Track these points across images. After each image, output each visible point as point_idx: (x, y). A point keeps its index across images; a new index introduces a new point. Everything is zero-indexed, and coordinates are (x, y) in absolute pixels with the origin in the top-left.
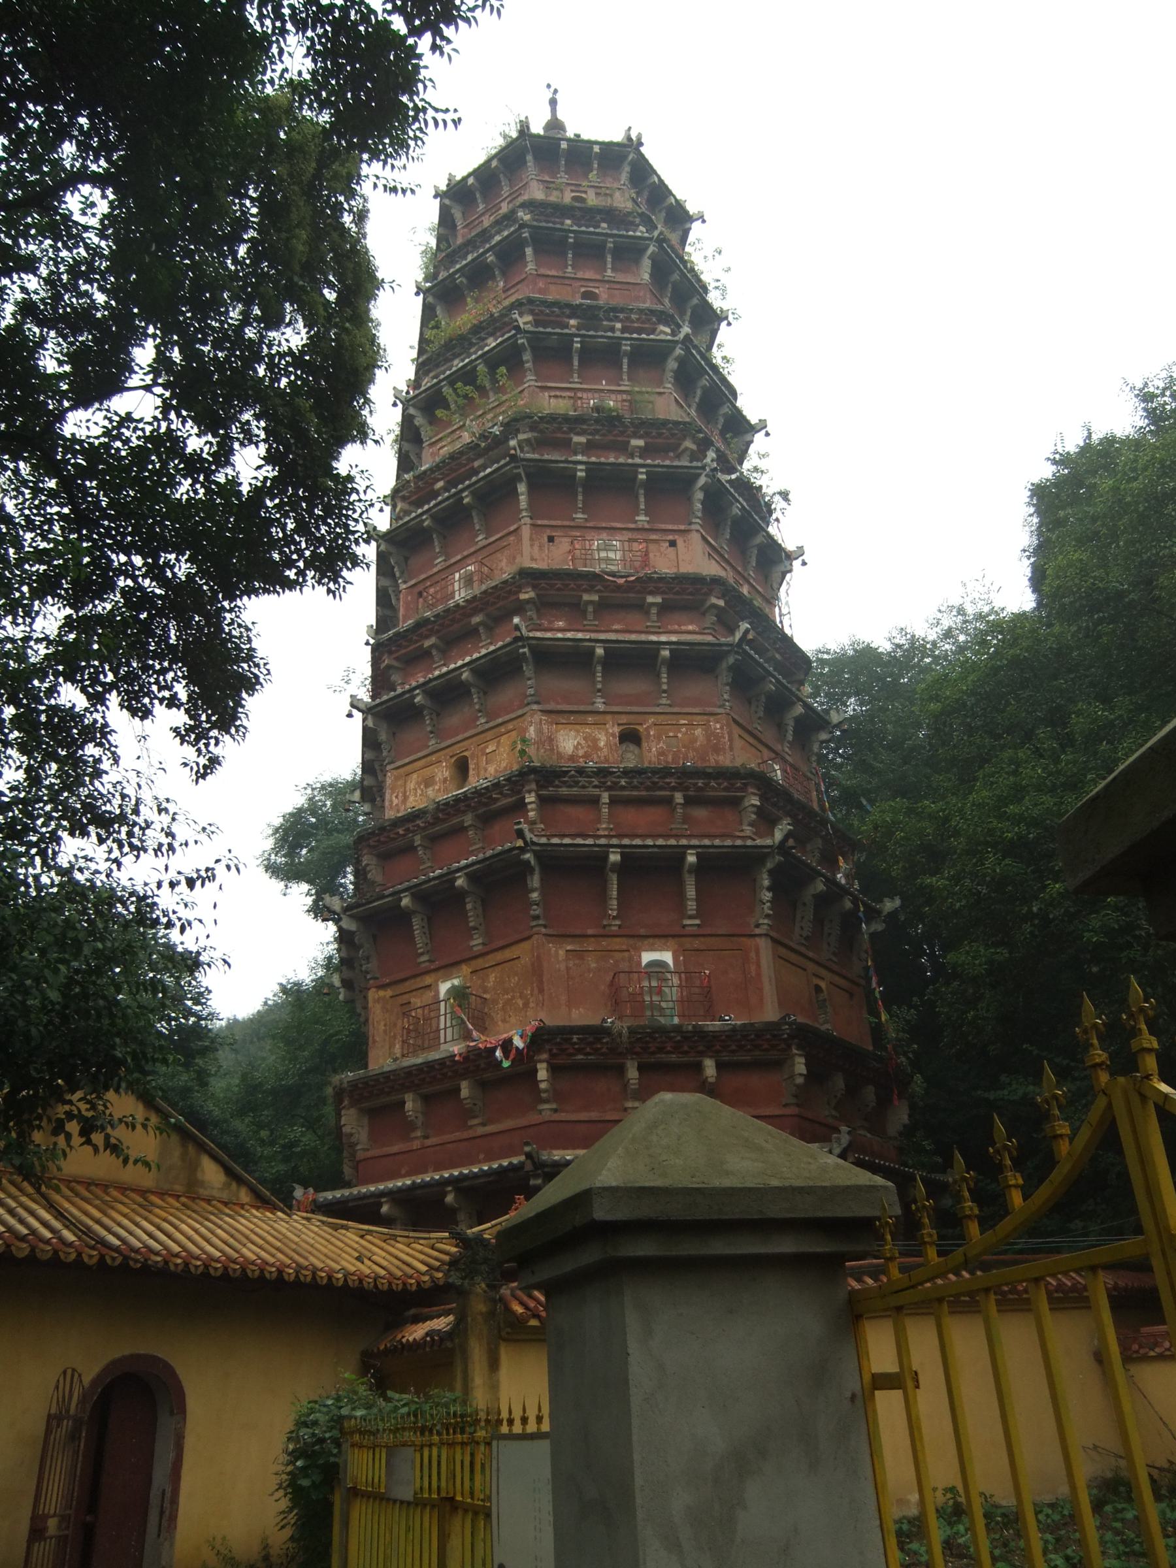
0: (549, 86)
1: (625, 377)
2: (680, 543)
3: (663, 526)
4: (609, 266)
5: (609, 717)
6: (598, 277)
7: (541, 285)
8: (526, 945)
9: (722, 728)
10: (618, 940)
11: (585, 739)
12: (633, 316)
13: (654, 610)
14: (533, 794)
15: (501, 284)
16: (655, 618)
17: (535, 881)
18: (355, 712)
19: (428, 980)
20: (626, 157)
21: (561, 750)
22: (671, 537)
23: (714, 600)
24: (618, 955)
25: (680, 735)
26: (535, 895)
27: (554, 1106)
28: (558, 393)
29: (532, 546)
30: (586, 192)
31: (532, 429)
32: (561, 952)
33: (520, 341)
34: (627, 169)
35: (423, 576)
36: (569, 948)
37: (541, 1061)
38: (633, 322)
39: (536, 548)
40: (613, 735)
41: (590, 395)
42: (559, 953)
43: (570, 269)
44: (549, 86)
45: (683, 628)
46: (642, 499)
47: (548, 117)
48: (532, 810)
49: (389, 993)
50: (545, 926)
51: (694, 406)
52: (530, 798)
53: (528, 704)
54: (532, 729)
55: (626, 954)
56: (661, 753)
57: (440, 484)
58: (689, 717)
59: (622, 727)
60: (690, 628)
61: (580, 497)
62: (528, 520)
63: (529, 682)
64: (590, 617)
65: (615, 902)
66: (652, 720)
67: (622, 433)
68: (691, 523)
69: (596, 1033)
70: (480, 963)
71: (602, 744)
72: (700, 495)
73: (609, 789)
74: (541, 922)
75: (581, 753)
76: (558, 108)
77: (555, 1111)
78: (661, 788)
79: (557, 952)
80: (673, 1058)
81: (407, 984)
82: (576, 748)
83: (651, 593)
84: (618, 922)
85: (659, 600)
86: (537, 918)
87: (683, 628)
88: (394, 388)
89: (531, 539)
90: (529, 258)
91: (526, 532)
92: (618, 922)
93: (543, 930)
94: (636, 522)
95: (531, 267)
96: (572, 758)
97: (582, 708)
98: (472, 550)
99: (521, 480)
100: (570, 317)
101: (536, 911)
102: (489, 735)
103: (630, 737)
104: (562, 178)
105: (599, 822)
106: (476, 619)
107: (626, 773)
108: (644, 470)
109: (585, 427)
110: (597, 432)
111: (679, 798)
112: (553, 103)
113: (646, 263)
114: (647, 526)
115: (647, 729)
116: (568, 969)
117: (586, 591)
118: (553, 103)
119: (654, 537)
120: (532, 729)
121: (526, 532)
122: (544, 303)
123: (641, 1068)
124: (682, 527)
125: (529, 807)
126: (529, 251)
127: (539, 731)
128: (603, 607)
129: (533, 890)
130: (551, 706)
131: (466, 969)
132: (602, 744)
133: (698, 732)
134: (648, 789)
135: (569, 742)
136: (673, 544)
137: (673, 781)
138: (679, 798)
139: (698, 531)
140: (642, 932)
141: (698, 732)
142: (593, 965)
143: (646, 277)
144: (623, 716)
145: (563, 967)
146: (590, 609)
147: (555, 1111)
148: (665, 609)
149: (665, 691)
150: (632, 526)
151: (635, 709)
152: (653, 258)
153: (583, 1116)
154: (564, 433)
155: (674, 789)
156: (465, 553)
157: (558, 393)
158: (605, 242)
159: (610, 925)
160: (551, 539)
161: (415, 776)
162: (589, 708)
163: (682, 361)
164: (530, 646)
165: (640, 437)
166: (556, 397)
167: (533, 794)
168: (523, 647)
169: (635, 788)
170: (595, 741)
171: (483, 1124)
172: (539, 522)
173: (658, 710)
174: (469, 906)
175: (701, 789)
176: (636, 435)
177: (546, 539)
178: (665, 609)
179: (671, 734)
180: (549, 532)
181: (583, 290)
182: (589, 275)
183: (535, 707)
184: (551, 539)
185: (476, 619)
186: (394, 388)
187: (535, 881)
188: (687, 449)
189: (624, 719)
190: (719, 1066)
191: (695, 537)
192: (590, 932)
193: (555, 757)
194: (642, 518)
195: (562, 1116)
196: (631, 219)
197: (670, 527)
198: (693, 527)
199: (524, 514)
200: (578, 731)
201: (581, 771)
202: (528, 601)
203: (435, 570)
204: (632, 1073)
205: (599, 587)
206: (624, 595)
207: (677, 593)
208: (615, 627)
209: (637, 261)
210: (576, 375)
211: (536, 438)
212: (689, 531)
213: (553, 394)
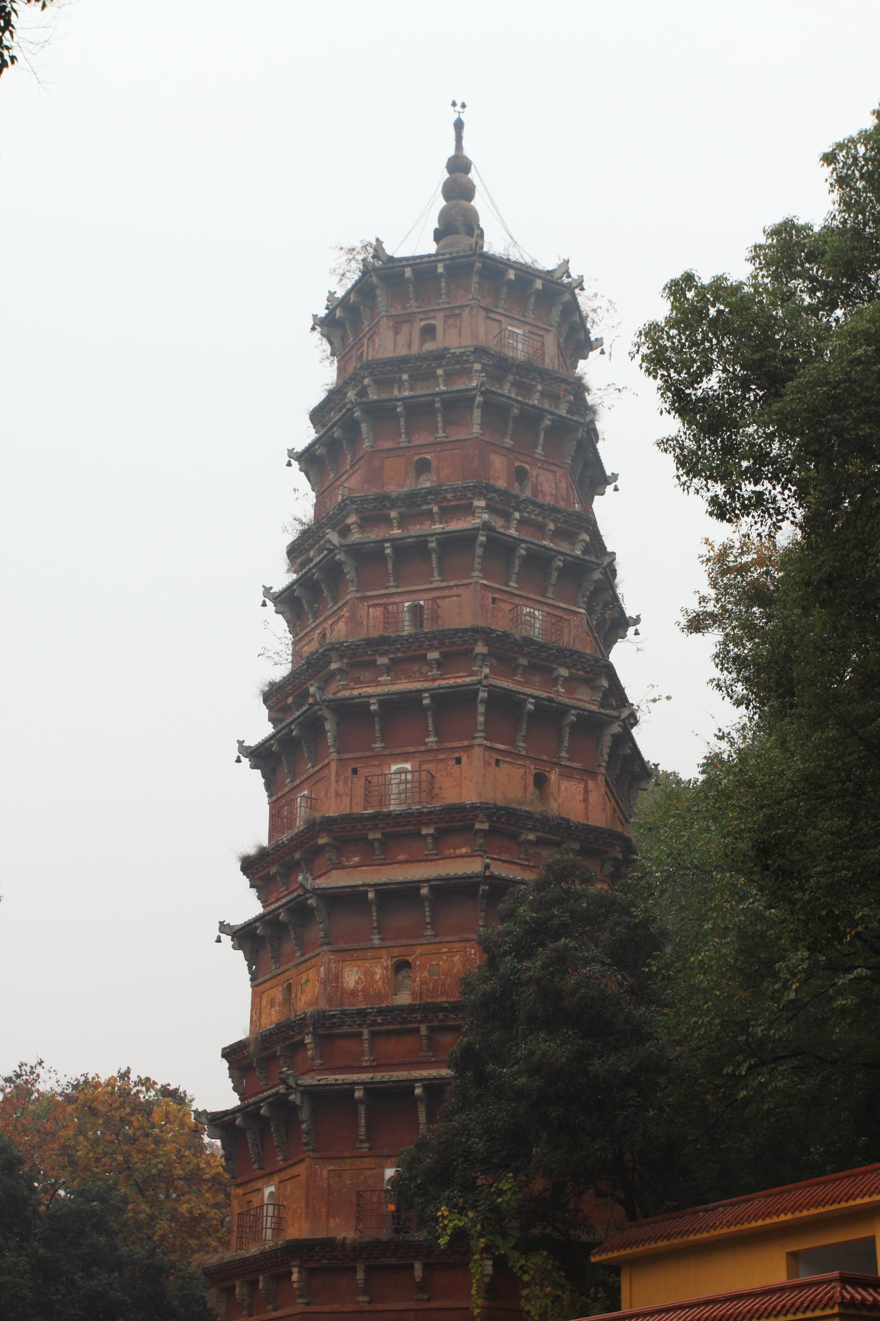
0: (454, 104)
1: (436, 573)
2: (464, 760)
3: (449, 745)
4: (440, 426)
5: (384, 951)
6: (431, 440)
7: (376, 463)
8: (304, 1165)
9: (475, 953)
10: (367, 1160)
11: (365, 974)
12: (449, 496)
13: (430, 840)
14: (310, 1036)
15: (349, 457)
16: (431, 847)
17: (305, 1114)
18: (224, 937)
19: (259, 1184)
20: (472, 265)
21: (345, 986)
22: (457, 755)
23: (478, 826)
24: (368, 1173)
25: (441, 963)
26: (304, 1126)
27: (306, 1301)
28: (376, 602)
29: (337, 782)
30: (435, 317)
31: (341, 657)
32: (325, 1172)
33: (338, 557)
34: (475, 279)
35: (280, 794)
36: (331, 1168)
37: (295, 1266)
38: (450, 501)
39: (341, 783)
40: (386, 968)
41: (403, 599)
42: (324, 1171)
43: (403, 438)
44: (454, 104)
45: (458, 852)
46: (430, 721)
47: (452, 152)
48: (311, 1049)
49: (240, 1191)
50: (314, 1151)
51: (514, 577)
52: (308, 1040)
53: (321, 945)
54: (322, 969)
55: (374, 1171)
56: (424, 982)
57: (290, 700)
58: (450, 945)
59: (394, 960)
60: (464, 850)
61: (377, 727)
62: (334, 756)
63: (321, 926)
64: (377, 852)
65: (363, 1129)
66: (419, 950)
67: (420, 647)
68: (474, 738)
69: (327, 1245)
70: (284, 1175)
71: (378, 977)
72: (481, 709)
73: (370, 1025)
74: (310, 1147)
75: (360, 987)
76: (466, 134)
77: (308, 1304)
78: (411, 1022)
79: (321, 1171)
80: (393, 1261)
81: (250, 1185)
82: (357, 983)
83: (426, 824)
84: (367, 1145)
85: (431, 831)
86: (307, 1144)
87: (458, 852)
88: (264, 586)
89: (337, 775)
90: (364, 435)
91: (333, 766)
92: (367, 1145)
93: (311, 1154)
94: (426, 744)
95: (367, 444)
96: (354, 993)
97: (362, 945)
98: (305, 776)
99: (327, 719)
100: (391, 509)
101: (305, 1139)
102: (303, 967)
103: (402, 965)
104: (413, 306)
105: (364, 1056)
106: (297, 856)
107: (380, 1011)
108: (427, 695)
109: (386, 648)
110: (398, 650)
111: (424, 1030)
112: (459, 126)
113: (477, 413)
114: (435, 747)
115: (414, 960)
116: (329, 1186)
117: (370, 829)
118: (459, 126)
119: (442, 756)
120: (322, 969)
121: (333, 766)
122: (364, 500)
123: (370, 1270)
124: (466, 743)
125: (308, 1046)
126: (364, 427)
127: (328, 970)
128: (388, 840)
129: (303, 1122)
130: (337, 947)
131: (276, 1179)
132: (378, 977)
133: (456, 958)
134: (400, 1023)
135: (351, 978)
136: (458, 761)
137: (419, 1016)
138: (424, 1030)
139: (480, 745)
140: (386, 1151)
141: (456, 958)
142: (348, 1182)
143: (476, 429)
144: (396, 950)
145: (325, 1185)
146: (377, 845)
147: (308, 1304)
148: (441, 835)
149: (429, 924)
150: (423, 748)
151: (405, 942)
152: (486, 407)
153: (327, 1308)
154: (370, 655)
155: (421, 1022)
156: (302, 778)
157: (376, 602)
158: (433, 403)
159: (362, 1148)
160: (355, 771)
161: (265, 995)
162: (368, 945)
163: (487, 546)
164: (317, 895)
165: (437, 648)
166: (375, 606)
167: (310, 1036)
168: (311, 897)
169: (389, 1024)
170: (373, 974)
171: (275, 1310)
172: (344, 756)
173: (423, 941)
174: (273, 1129)
175: (440, 1020)
176: (431, 648)
177: (350, 771)
178: (441, 835)
179: (434, 963)
180: (353, 765)
181: (416, 458)
182: (420, 439)
183: (325, 948)
184: (355, 771)
185: (297, 856)
186: (264, 586)
187: (305, 1114)
188: (477, 654)
189: (396, 951)
190: (426, 1267)
191: (477, 752)
192: (346, 1154)
193: (339, 993)
194: (432, 739)
195: (312, 1308)
196: (465, 358)
197: (455, 744)
198: (476, 742)
199: (332, 750)
200: (359, 967)
201: (344, 1013)
202: (326, 845)
203: (286, 789)
204: (360, 1275)
205: (380, 826)
206: (395, 832)
207: (447, 822)
208: (401, 857)
209: (471, 408)
210: (391, 579)
211: (347, 664)
212: (471, 746)
213: (371, 603)
